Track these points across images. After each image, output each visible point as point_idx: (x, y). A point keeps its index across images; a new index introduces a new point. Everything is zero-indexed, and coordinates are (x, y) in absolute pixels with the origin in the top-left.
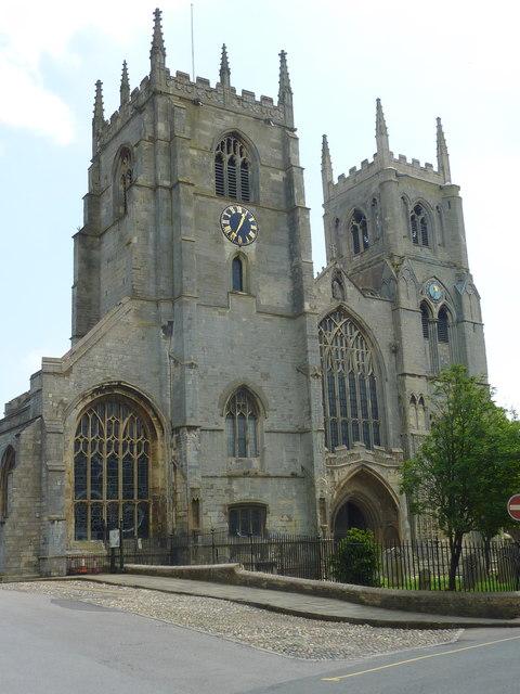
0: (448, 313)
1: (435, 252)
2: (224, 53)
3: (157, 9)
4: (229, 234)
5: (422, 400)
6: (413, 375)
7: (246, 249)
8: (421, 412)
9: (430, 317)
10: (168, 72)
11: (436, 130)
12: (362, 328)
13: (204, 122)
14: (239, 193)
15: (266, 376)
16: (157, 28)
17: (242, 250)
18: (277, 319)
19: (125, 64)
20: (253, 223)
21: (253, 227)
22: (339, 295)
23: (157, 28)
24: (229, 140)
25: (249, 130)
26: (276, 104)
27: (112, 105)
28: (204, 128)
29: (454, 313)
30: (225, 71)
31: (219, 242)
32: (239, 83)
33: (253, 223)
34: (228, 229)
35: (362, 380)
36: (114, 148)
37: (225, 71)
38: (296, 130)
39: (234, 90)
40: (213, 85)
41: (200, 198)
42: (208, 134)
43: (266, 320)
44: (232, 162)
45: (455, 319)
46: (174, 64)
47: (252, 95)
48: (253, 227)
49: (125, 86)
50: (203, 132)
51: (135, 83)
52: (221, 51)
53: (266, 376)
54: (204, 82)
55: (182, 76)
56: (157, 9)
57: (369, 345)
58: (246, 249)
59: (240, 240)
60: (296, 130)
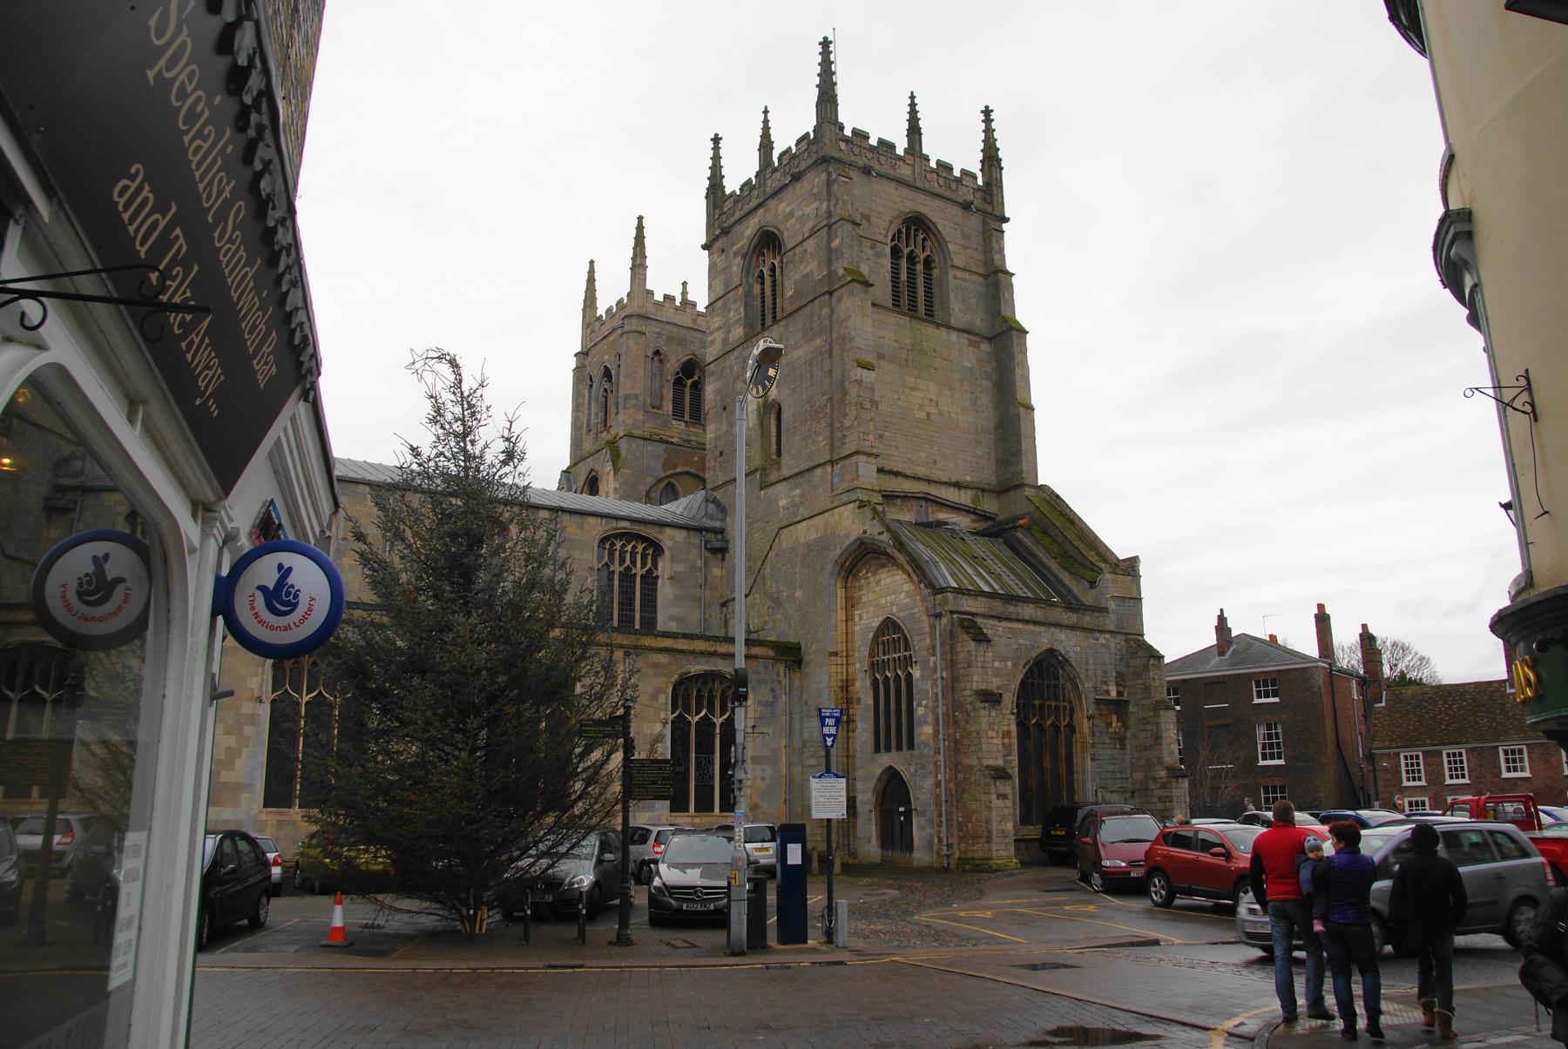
2: (913, 105)
10: (842, 128)
19: (766, 112)
25: (943, 217)
26: (980, 182)
27: (740, 170)
30: (914, 131)
32: (935, 149)
36: (749, 229)
37: (914, 131)
38: (1007, 220)
39: (927, 159)
40: (900, 151)
46: (850, 117)
47: (949, 168)
49: (766, 145)
51: (784, 140)
52: (909, 101)
54: (886, 146)
55: (861, 136)
60: (1007, 220)
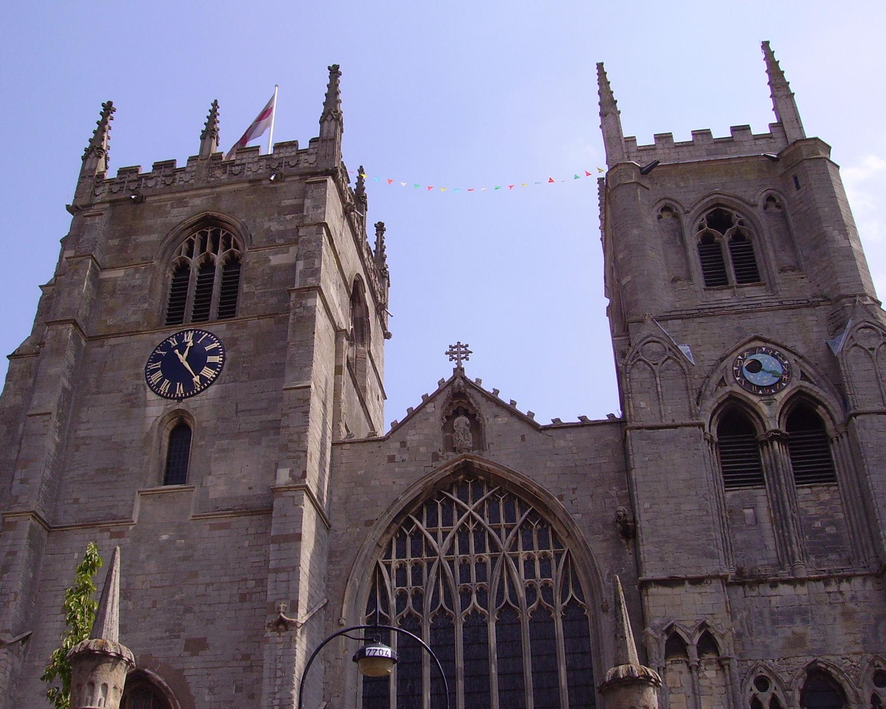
0: (820, 410)
1: (772, 288)
3: (110, 103)
4: (159, 385)
5: (708, 643)
6: (672, 582)
7: (192, 404)
8: (710, 673)
9: (760, 432)
11: (764, 66)
12: (535, 499)
13: (149, 222)
14: (214, 310)
15: (197, 646)
16: (102, 126)
17: (181, 406)
18: (245, 521)
20: (214, 352)
21: (210, 359)
22: (466, 440)
23: (102, 126)
24: (204, 236)
28: (150, 230)
29: (834, 405)
31: (134, 402)
33: (214, 352)
34: (156, 377)
35: (542, 618)
41: (113, 341)
42: (154, 237)
43: (213, 527)
44: (207, 266)
45: (839, 417)
48: (210, 359)
50: (142, 239)
53: (197, 646)
56: (110, 103)
57: (563, 537)
58: (192, 404)
59: (180, 389)
